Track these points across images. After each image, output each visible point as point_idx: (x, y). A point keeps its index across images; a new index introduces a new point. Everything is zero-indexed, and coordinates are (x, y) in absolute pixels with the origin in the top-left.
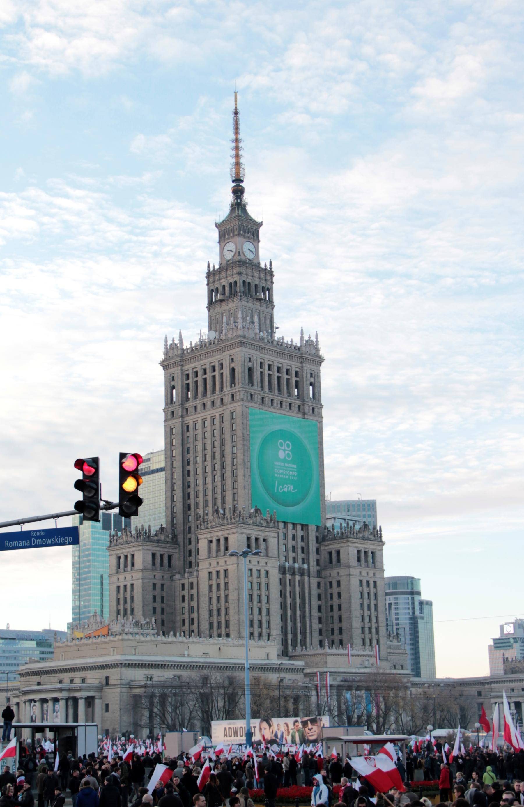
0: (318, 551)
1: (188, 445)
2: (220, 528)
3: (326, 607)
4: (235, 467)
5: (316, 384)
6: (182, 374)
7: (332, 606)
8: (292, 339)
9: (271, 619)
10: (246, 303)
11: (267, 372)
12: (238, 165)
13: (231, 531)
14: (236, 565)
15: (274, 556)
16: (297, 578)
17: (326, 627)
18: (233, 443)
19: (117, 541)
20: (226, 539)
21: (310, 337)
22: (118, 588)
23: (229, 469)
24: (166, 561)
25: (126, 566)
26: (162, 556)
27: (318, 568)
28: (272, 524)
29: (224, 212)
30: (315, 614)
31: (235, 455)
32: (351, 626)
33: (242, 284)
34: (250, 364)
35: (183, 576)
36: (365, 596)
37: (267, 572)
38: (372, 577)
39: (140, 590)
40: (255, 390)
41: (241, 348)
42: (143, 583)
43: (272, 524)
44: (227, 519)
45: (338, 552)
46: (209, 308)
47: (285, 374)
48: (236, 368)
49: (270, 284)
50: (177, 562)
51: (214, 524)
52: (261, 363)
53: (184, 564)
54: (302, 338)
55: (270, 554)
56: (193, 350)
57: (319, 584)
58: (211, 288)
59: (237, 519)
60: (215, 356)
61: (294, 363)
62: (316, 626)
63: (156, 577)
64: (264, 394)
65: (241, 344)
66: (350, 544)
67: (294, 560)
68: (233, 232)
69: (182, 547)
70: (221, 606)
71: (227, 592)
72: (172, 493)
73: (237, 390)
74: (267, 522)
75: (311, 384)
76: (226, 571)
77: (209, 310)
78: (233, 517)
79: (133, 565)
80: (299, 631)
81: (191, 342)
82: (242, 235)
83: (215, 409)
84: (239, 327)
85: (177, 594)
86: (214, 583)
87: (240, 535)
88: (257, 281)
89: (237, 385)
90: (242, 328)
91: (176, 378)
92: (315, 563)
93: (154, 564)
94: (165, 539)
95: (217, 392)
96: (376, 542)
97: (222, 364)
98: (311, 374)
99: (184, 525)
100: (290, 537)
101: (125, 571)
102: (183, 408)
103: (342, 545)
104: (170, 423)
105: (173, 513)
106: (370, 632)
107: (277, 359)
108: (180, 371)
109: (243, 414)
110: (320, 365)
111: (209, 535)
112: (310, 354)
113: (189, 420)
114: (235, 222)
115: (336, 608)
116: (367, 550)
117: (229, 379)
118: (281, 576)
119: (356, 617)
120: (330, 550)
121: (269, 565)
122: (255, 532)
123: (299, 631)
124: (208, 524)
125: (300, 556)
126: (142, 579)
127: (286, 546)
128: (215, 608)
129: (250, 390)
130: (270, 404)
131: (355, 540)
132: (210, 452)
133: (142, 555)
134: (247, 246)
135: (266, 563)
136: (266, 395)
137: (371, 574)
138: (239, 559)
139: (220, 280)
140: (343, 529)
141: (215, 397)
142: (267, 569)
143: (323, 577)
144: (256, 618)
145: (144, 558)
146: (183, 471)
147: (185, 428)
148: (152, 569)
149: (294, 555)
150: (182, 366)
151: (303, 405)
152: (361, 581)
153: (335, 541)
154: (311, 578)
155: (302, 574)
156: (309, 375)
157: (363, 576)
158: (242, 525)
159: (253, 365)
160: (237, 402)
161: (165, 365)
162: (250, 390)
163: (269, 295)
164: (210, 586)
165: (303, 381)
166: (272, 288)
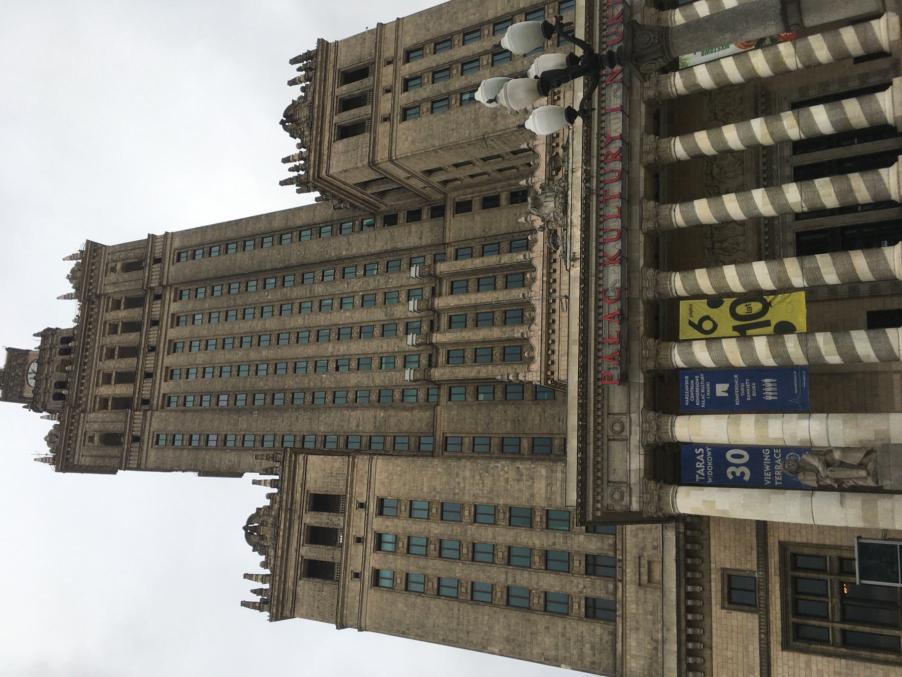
0: (390, 220)
5: (123, 255)
9: (502, 502)
27: (425, 215)
36: (440, 87)
38: (395, 71)
92: (414, 227)
121: (363, 499)
142: (373, 507)
144: (498, 576)
151: (152, 289)
152: (405, 114)
156: (112, 277)
159: (96, 431)
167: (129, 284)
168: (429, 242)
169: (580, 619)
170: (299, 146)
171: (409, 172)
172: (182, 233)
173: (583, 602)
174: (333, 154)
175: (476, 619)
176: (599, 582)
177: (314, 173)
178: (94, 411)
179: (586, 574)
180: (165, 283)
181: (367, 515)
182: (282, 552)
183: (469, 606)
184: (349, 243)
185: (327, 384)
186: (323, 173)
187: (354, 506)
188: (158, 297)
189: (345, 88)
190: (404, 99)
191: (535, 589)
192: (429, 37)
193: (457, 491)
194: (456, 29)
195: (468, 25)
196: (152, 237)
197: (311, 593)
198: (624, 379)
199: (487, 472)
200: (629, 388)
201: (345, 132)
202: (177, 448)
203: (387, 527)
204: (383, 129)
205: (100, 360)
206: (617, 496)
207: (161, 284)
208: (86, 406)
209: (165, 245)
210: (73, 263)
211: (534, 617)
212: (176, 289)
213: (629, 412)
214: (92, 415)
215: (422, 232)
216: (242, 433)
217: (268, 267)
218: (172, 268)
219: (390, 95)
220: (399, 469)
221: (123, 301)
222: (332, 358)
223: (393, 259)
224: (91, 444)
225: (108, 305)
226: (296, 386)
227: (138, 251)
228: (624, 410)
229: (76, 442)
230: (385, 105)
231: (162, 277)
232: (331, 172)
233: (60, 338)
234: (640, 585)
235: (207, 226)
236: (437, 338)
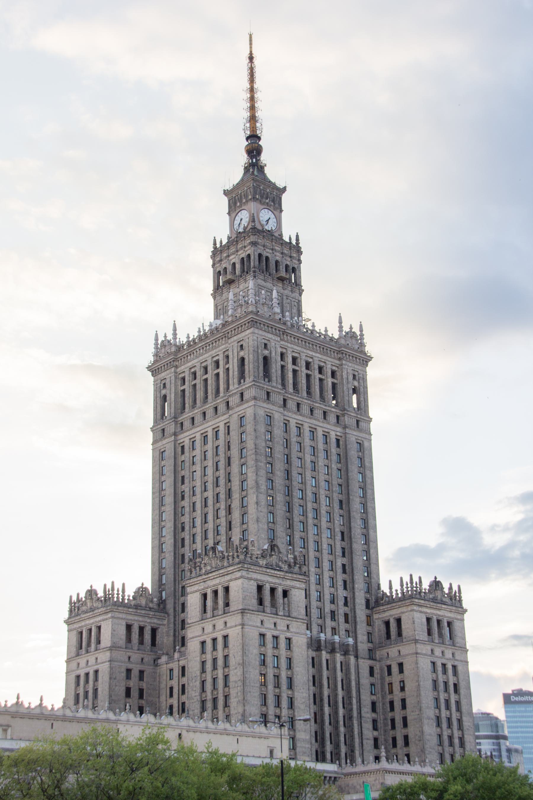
1: (183, 473)
2: (217, 573)
3: (383, 704)
4: (244, 493)
5: (362, 390)
6: (176, 378)
7: (392, 703)
8: (326, 328)
10: (263, 282)
11: (290, 367)
12: (253, 119)
13: (233, 576)
14: (240, 627)
15: (300, 617)
16: (339, 657)
17: (384, 735)
18: (242, 460)
19: (78, 610)
20: (227, 589)
21: (351, 328)
22: (78, 677)
23: (236, 496)
24: (148, 636)
25: (89, 644)
26: (141, 629)
27: (370, 645)
28: (296, 569)
29: (235, 174)
30: (367, 714)
31: (245, 476)
32: (422, 732)
33: (257, 257)
34: (266, 352)
35: (171, 658)
37: (289, 640)
38: (450, 659)
39: (107, 678)
40: (273, 387)
41: (252, 329)
42: (111, 668)
43: (296, 569)
44: (228, 559)
45: (399, 621)
46: (214, 296)
47: (317, 371)
48: (246, 357)
49: (297, 262)
50: (165, 638)
51: (209, 568)
52: (282, 355)
53: (174, 641)
54: (341, 328)
55: (294, 614)
56: (191, 344)
57: (371, 669)
58: (218, 270)
59: (242, 557)
60: (219, 346)
61: (329, 359)
62: (369, 734)
63: (131, 660)
64: (287, 395)
65: (254, 323)
66: (415, 608)
67: (334, 631)
68: (246, 196)
69: (172, 617)
70: (218, 694)
71: (226, 670)
72: (160, 540)
73: (247, 386)
74: (290, 566)
75: (355, 391)
76: (225, 637)
77: (215, 298)
78: (236, 554)
79: (99, 642)
80: (342, 739)
81: (188, 334)
82: (257, 199)
83: (218, 417)
84: (250, 302)
85: (163, 686)
86: (209, 657)
87: (246, 581)
88: (279, 257)
89: (247, 379)
90: (254, 302)
91: (168, 386)
92: (365, 638)
93: (129, 639)
94: (146, 604)
95: (222, 394)
96: (454, 608)
97: (227, 357)
98: (354, 376)
99: (175, 584)
100: (327, 597)
101: (87, 652)
102: (176, 423)
103: (404, 609)
104: (160, 444)
105: (161, 568)
106: (451, 744)
107: (305, 351)
108: (173, 374)
109: (255, 418)
110: (367, 365)
111: (202, 586)
112: (353, 350)
113: (185, 438)
114: (248, 184)
115: (398, 705)
116: (440, 618)
117: (236, 373)
118: (314, 654)
119: (429, 718)
120: (387, 619)
122: (270, 579)
123: (342, 739)
124: (201, 569)
125: (343, 626)
126: (110, 661)
127: (321, 610)
128: (209, 697)
129: (265, 386)
130: (295, 408)
131: (422, 602)
132: (212, 477)
133: (110, 625)
134: (265, 215)
135: (288, 626)
136: (289, 396)
137: (448, 654)
138: (245, 618)
139: (228, 256)
140: (405, 586)
141: (218, 401)
142: (289, 635)
143: (378, 659)
145: (113, 630)
146: (175, 509)
147: (180, 449)
148: (126, 648)
149: (334, 624)
150: (177, 367)
151: (343, 415)
152: (434, 663)
153: (394, 605)
154: (359, 660)
155: (346, 653)
156: (351, 377)
157: (437, 657)
158: (249, 566)
159: (271, 353)
160: (247, 402)
161: (154, 370)
162: (265, 386)
163: (295, 277)
164: (203, 663)
165: (343, 384)
166: (299, 268)
168: (359, 648)
170: (425, 589)
174: (421, 614)
175: (255, 697)
184: (360, 590)
192: (460, 681)
194: (461, 697)
195: (462, 705)
196: (370, 420)
204: (429, 648)
212: (341, 437)
218: (353, 439)
219: (441, 655)
222: (307, 569)
224: (263, 346)
226: (295, 540)
232: (415, 613)
236: (324, 653)
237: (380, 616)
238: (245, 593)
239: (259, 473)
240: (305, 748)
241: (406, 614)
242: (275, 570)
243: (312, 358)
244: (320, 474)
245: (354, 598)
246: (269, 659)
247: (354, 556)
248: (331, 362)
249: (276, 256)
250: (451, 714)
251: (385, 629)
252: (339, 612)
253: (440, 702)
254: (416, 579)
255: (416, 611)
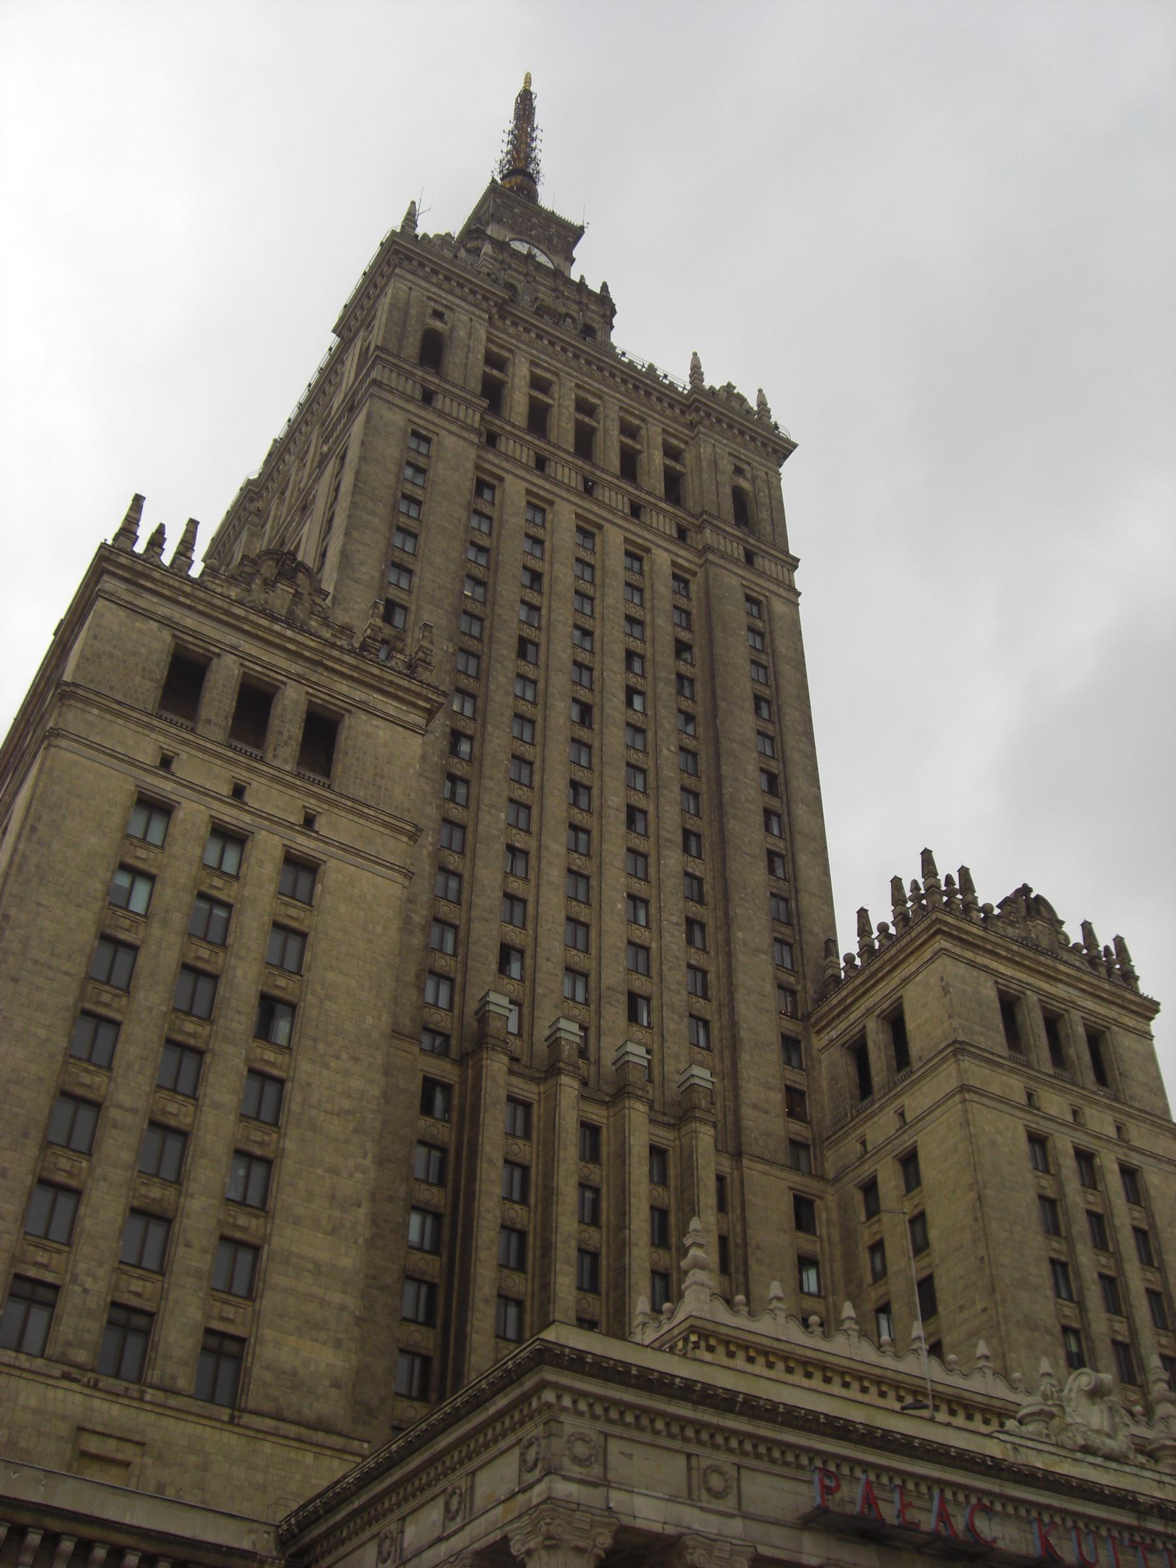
5: (763, 498)
9: (290, 1145)
27: (796, 1127)
34: (438, 325)
38: (1108, 1140)
45: (896, 1022)
57: (803, 1212)
92: (777, 1098)
116: (1055, 1006)
121: (321, 824)
143: (831, 1176)
151: (700, 529)
152: (1037, 1140)
154: (745, 1162)
156: (727, 465)
157: (1051, 1119)
159: (453, 329)
167: (709, 486)
168: (747, 1123)
169: (15, 1260)
170: (987, 909)
171: (920, 1119)
172: (796, 623)
173: (49, 1277)
174: (975, 973)
176: (94, 1328)
177: (946, 923)
178: (489, 340)
179: (114, 1304)
180: (710, 556)
181: (291, 826)
182: (237, 617)
183: (71, 1001)
184: (756, 951)
185: (486, 818)
186: (945, 944)
187: (312, 803)
188: (682, 534)
189: (1081, 1030)
190: (1063, 1144)
191: (91, 1170)
193: (321, 1047)
196: (793, 563)
197: (143, 650)
198: (819, 1521)
199: (355, 1131)
200: (792, 1526)
201: (1009, 1006)
202: (401, 470)
203: (261, 863)
204: (1014, 1086)
205: (577, 386)
206: (581, 1449)
207: (707, 548)
208: (498, 329)
209: (779, 583)
210: (753, 403)
211: (32, 1150)
212: (694, 574)
213: (745, 1516)
214: (483, 333)
215: (766, 1112)
216: (413, 607)
217: (726, 770)
218: (735, 581)
219: (1069, 1118)
220: (379, 929)
221: (678, 467)
223: (715, 1033)
224: (430, 311)
225: (675, 437)
226: (489, 749)
227: (769, 528)
228: (748, 1507)
229: (436, 285)
230: (1055, 1104)
231: (723, 555)
232: (947, 961)
233: (596, 326)
234: (81, 1429)
235: (804, 675)
237: (834, 1034)
238: (97, 644)
239: (355, 534)
240: (323, 1303)
241: (919, 978)
242: (274, 619)
243: (601, 398)
244: (609, 625)
245: (730, 972)
246: (169, 891)
247: (731, 852)
248: (663, 423)
249: (535, 290)
250: (1133, 1331)
251: (853, 1071)
252: (666, 999)
253: (1078, 1276)
254: (946, 867)
255: (956, 958)
